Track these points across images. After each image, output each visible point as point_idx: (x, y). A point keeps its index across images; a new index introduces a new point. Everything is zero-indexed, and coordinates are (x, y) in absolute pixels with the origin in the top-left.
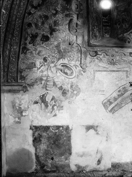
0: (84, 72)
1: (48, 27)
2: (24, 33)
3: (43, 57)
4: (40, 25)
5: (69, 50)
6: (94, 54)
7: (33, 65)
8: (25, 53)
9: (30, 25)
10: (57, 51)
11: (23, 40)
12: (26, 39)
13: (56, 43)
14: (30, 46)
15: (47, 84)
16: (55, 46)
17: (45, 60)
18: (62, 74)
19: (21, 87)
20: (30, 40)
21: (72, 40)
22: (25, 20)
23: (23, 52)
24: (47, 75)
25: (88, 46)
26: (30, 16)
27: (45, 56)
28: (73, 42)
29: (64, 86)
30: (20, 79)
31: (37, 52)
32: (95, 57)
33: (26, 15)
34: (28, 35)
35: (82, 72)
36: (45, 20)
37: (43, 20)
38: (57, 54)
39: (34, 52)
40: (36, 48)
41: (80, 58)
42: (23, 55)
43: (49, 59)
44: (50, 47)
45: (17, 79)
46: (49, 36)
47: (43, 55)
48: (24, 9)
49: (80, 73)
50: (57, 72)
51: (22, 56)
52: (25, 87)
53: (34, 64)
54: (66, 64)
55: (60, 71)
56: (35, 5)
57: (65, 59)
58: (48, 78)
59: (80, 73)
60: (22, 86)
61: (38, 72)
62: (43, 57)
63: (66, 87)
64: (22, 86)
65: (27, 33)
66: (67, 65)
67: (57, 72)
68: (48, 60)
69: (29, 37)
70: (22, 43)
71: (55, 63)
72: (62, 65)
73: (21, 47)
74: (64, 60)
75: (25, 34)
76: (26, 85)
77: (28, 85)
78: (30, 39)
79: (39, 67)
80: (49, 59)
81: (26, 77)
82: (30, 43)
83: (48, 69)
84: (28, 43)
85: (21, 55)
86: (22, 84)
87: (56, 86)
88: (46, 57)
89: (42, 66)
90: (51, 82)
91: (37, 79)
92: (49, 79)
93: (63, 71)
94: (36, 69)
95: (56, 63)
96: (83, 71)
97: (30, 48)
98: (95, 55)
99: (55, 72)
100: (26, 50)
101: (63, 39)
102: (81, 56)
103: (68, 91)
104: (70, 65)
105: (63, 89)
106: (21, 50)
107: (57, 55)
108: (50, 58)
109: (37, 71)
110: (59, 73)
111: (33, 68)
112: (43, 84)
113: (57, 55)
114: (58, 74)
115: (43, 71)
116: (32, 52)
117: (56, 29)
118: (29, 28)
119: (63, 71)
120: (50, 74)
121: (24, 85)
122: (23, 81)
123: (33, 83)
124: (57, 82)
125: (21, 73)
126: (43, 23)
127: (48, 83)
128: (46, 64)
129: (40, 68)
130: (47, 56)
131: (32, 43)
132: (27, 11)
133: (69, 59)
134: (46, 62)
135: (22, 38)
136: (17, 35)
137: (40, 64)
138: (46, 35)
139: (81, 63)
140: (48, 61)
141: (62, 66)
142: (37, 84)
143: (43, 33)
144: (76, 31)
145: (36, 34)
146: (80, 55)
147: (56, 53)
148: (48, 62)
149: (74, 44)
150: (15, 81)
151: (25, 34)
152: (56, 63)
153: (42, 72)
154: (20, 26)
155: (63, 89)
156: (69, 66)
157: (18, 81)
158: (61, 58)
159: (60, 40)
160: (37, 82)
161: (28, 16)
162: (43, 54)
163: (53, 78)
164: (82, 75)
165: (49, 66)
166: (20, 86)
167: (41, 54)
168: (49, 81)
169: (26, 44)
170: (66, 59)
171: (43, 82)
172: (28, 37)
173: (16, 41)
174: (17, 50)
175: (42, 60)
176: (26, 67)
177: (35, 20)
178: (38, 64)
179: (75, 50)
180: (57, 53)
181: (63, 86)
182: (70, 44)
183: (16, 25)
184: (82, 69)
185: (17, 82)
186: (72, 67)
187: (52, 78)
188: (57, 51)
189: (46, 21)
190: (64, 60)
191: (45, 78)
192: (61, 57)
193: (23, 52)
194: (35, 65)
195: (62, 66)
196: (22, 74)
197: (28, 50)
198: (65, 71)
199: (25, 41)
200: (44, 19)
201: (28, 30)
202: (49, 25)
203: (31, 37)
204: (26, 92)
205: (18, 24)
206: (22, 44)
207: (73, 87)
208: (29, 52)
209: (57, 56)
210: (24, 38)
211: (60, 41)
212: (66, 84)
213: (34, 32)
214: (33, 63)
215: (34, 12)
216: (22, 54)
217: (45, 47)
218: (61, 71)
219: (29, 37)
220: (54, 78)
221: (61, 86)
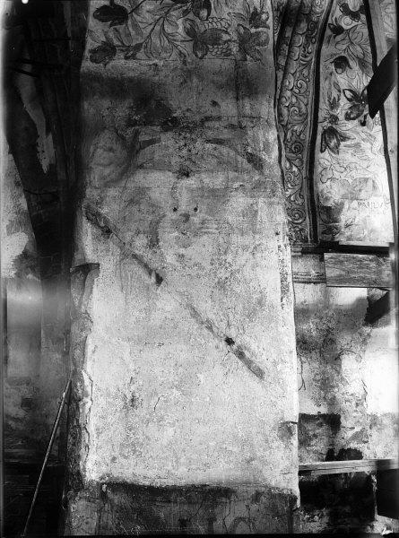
2: (324, 85)
8: (336, 150)
11: (324, 106)
12: (334, 104)
22: (324, 47)
23: (327, 145)
26: (339, 38)
33: (328, 32)
39: (365, 145)
40: (372, 133)
42: (326, 154)
48: (322, 12)
56: (351, 8)
65: (336, 85)
69: (342, 96)
70: (322, 114)
75: (330, 88)
78: (349, 105)
82: (348, 117)
84: (341, 117)
85: (321, 155)
97: (349, 134)
100: (338, 140)
106: (319, 137)
116: (357, 146)
118: (340, 71)
131: (354, 119)
132: (330, 21)
135: (321, 99)
136: (302, 91)
151: (330, 88)
169: (335, 119)
172: (339, 99)
177: (359, 49)
197: (345, 138)
199: (332, 108)
201: (338, 76)
205: (306, 57)
206: (320, 119)
210: (327, 102)
214: (366, 180)
215: (349, 27)
216: (322, 151)
219: (342, 96)
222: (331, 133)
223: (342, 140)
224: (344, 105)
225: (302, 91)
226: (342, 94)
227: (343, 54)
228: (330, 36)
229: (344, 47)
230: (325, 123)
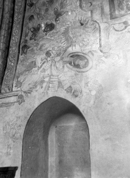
0: (106, 57)
1: (52, 13)
3: (45, 51)
4: (43, 13)
5: (81, 33)
6: (122, 26)
7: (33, 64)
8: (25, 53)
9: (31, 18)
10: (64, 38)
13: (63, 29)
14: (30, 43)
15: (49, 87)
16: (62, 33)
17: (48, 54)
18: (71, 67)
19: (16, 97)
20: (32, 35)
21: (85, 19)
24: (50, 74)
25: (111, 19)
26: (32, 8)
27: (48, 50)
28: (87, 20)
29: (75, 86)
30: (16, 86)
31: (39, 47)
32: (124, 31)
33: (27, 7)
34: (29, 30)
35: (103, 58)
36: (49, 6)
37: (46, 6)
38: (64, 43)
39: (35, 48)
41: (98, 40)
42: (23, 56)
43: (54, 51)
44: (56, 36)
45: (13, 87)
46: (54, 23)
47: (47, 48)
49: (100, 61)
50: (63, 67)
51: (21, 57)
52: (21, 97)
53: (34, 63)
54: (78, 52)
55: (68, 65)
57: (75, 46)
58: (52, 77)
59: (100, 61)
60: (17, 95)
61: (39, 73)
62: (45, 51)
63: (78, 86)
64: (17, 95)
66: (79, 54)
67: (63, 67)
68: (52, 54)
70: (22, 41)
71: (61, 56)
72: (71, 55)
73: (21, 47)
74: (74, 47)
76: (23, 94)
77: (25, 92)
79: (40, 65)
80: (54, 51)
81: (23, 82)
82: (31, 39)
83: (51, 65)
86: (18, 92)
87: (63, 88)
88: (50, 51)
89: (43, 63)
90: (54, 82)
91: (36, 83)
92: (52, 80)
93: (73, 63)
94: (36, 69)
95: (63, 55)
96: (105, 56)
97: (30, 45)
98: (124, 27)
99: (61, 67)
100: (27, 49)
101: (72, 22)
102: (100, 35)
103: (81, 92)
104: (83, 53)
105: (73, 91)
106: (21, 50)
107: (64, 44)
108: (54, 50)
109: (37, 71)
110: (67, 67)
111: (32, 69)
112: (43, 88)
113: (64, 44)
114: (66, 69)
115: (45, 70)
116: (33, 49)
117: (63, 11)
119: (73, 63)
120: (54, 72)
121: (20, 94)
122: (19, 89)
123: (31, 88)
124: (64, 81)
125: (18, 79)
126: (47, 10)
127: (51, 85)
128: (49, 59)
129: (41, 66)
130: (51, 49)
133: (81, 44)
134: (49, 57)
135: (23, 35)
137: (42, 60)
138: (50, 23)
139: (101, 46)
140: (52, 54)
141: (71, 57)
142: (36, 90)
143: (46, 22)
144: (91, 5)
145: (39, 26)
146: (98, 35)
147: (63, 41)
148: (52, 56)
149: (88, 22)
150: (9, 90)
152: (63, 55)
153: (44, 70)
154: (20, 22)
155: (73, 91)
156: (82, 54)
157: (13, 90)
158: (70, 46)
159: (69, 23)
160: (36, 86)
161: (30, 9)
162: (45, 47)
163: (58, 76)
164: (104, 62)
165: (53, 60)
166: (15, 96)
167: (43, 48)
168: (52, 81)
169: (26, 41)
170: (76, 45)
171: (44, 85)
173: (15, 41)
174: (17, 51)
175: (45, 56)
176: (24, 69)
178: (39, 63)
179: (89, 30)
180: (64, 42)
181: (72, 86)
182: (82, 24)
183: (15, 22)
184: (102, 54)
185: (12, 91)
186: (86, 54)
187: (57, 77)
188: (64, 38)
189: (50, 7)
190: (74, 47)
191: (47, 79)
192: (69, 45)
193: (23, 52)
194: (35, 64)
195: (71, 57)
196: (19, 79)
197: (29, 48)
198: (76, 63)
200: (48, 5)
202: (54, 9)
203: (32, 32)
204: (22, 103)
205: (18, 20)
207: (89, 85)
208: (30, 50)
209: (64, 45)
211: (68, 25)
212: (77, 82)
213: (35, 25)
214: (32, 62)
217: (49, 38)
218: (70, 63)
219: (30, 32)
220: (59, 77)
221: (70, 87)
222: (25, 47)
223: (28, 49)
224: (30, 34)
225: (17, 34)
226: (30, 30)
227: (33, 14)
228: (29, 8)
229: (33, 11)
230: (23, 44)
